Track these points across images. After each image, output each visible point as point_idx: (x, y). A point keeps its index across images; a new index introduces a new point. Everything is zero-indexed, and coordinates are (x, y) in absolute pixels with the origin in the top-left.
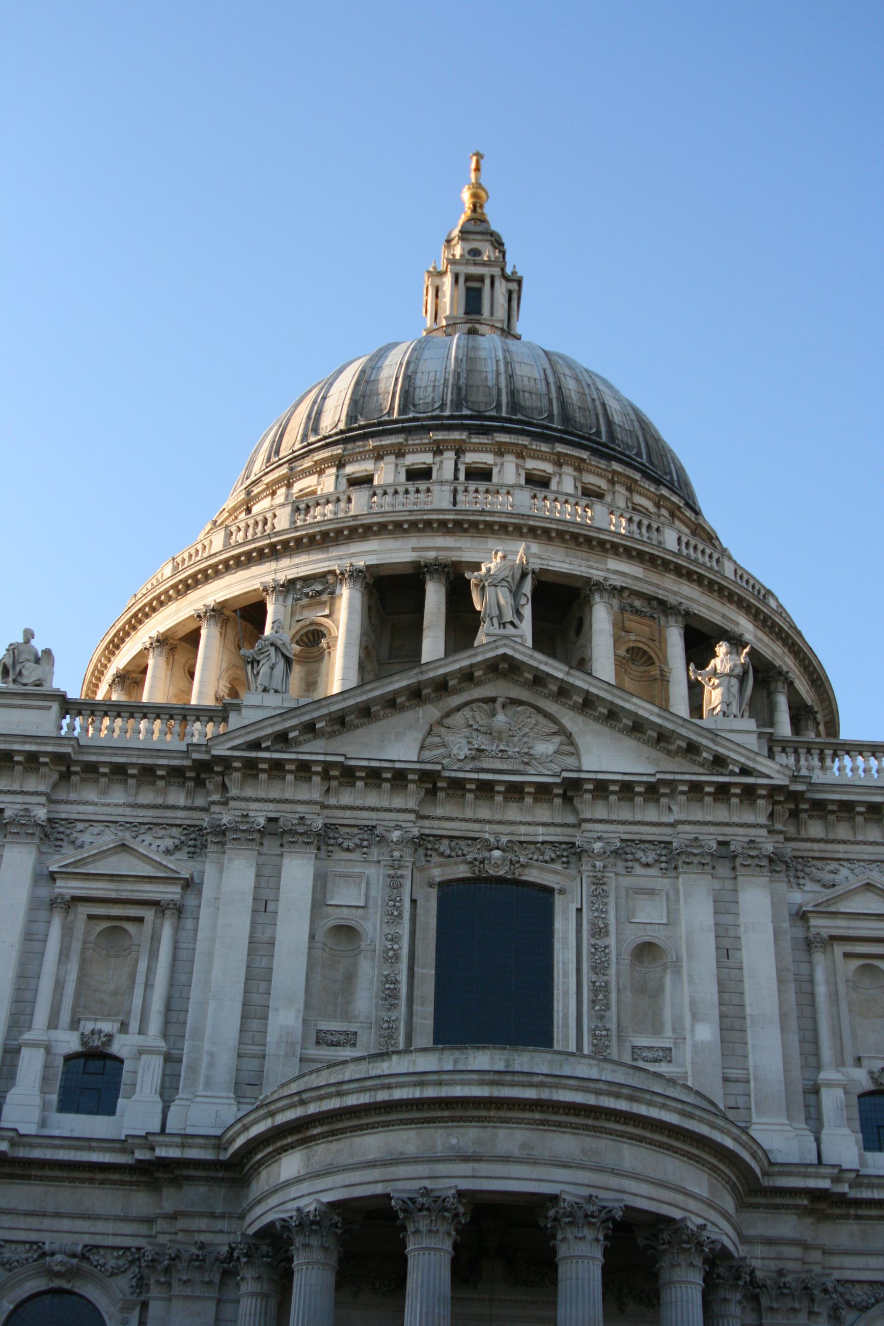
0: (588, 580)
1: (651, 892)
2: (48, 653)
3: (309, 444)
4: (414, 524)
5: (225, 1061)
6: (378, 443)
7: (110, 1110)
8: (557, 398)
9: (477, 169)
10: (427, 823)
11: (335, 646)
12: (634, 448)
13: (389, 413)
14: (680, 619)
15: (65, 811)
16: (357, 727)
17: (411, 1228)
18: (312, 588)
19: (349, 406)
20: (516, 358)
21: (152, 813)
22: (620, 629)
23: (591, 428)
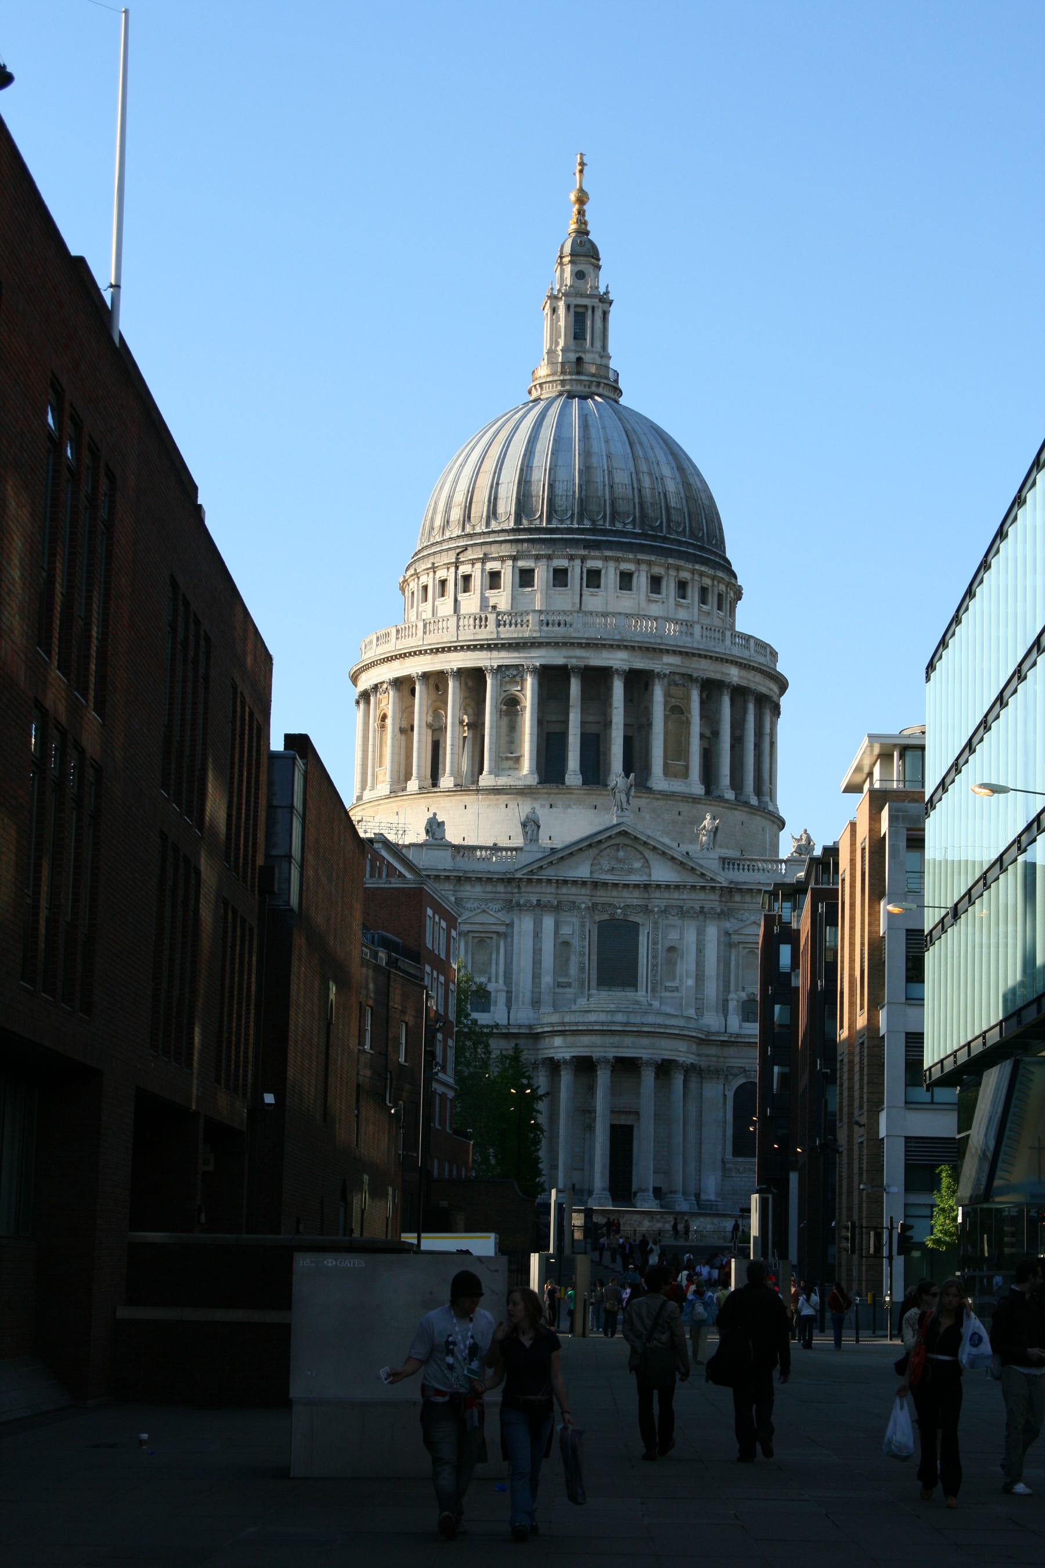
0: (653, 671)
1: (674, 926)
2: (443, 823)
3: (493, 532)
4: (565, 644)
5: (528, 995)
6: (537, 553)
7: (489, 1011)
8: (639, 503)
9: (581, 171)
10: (594, 898)
11: (525, 711)
12: (681, 523)
13: (541, 516)
14: (699, 685)
15: (460, 895)
16: (566, 859)
17: (599, 1067)
18: (511, 671)
19: (516, 504)
20: (615, 465)
21: (492, 895)
22: (667, 695)
23: (657, 520)
